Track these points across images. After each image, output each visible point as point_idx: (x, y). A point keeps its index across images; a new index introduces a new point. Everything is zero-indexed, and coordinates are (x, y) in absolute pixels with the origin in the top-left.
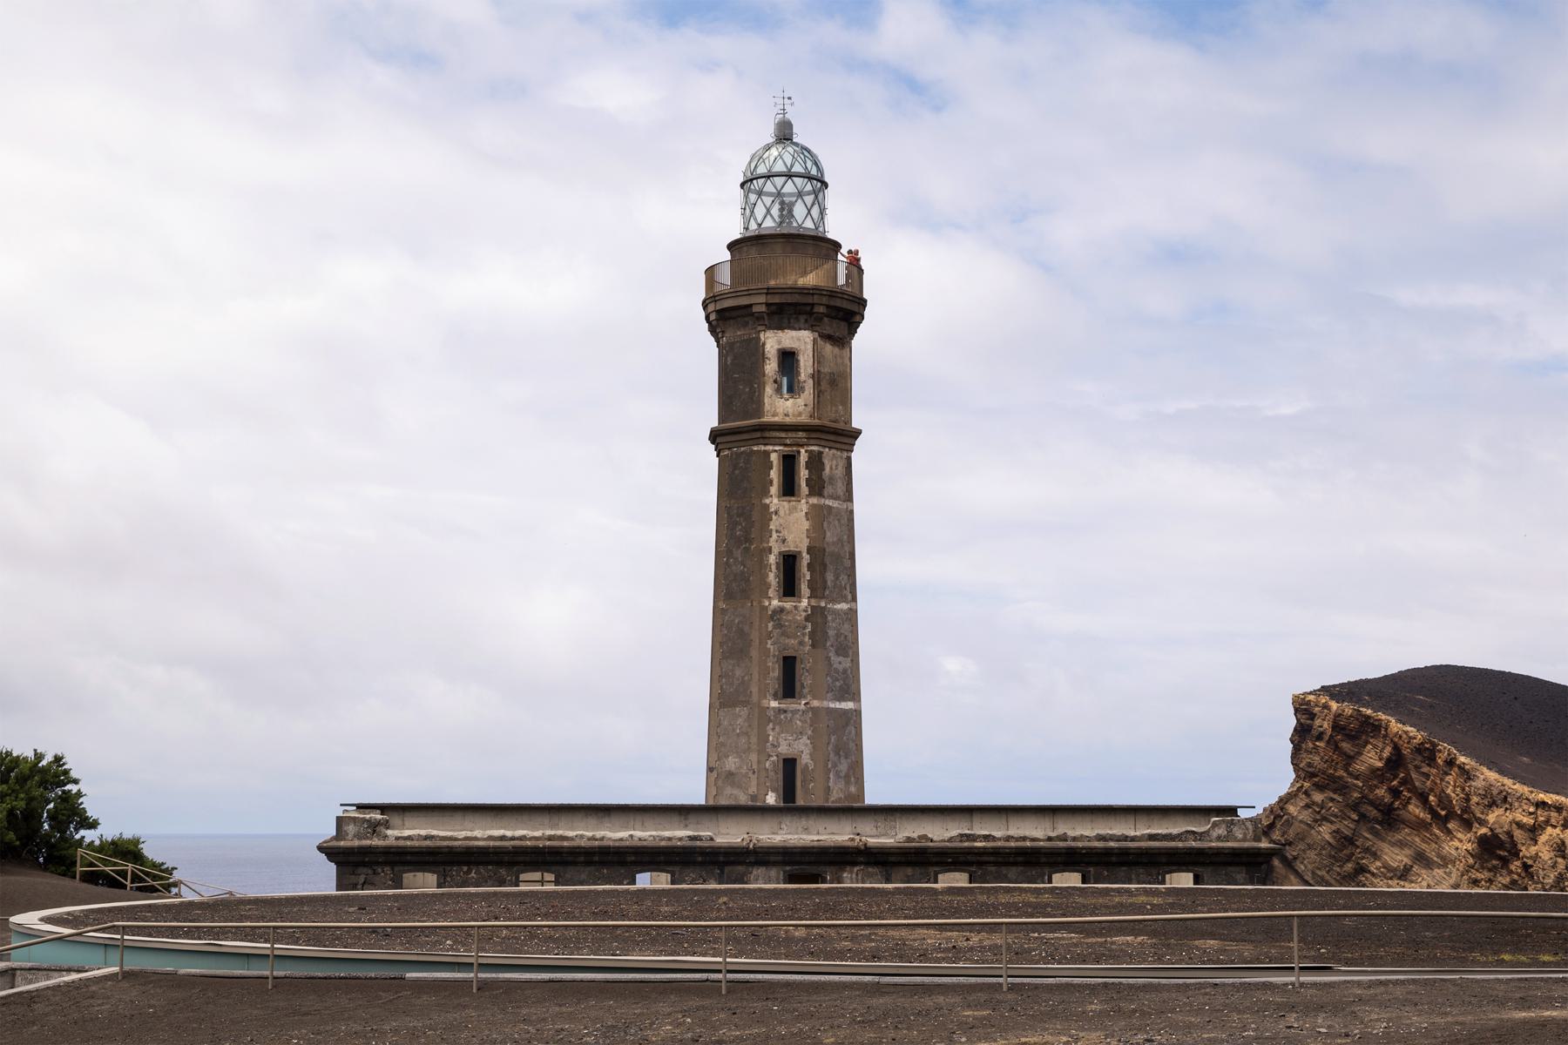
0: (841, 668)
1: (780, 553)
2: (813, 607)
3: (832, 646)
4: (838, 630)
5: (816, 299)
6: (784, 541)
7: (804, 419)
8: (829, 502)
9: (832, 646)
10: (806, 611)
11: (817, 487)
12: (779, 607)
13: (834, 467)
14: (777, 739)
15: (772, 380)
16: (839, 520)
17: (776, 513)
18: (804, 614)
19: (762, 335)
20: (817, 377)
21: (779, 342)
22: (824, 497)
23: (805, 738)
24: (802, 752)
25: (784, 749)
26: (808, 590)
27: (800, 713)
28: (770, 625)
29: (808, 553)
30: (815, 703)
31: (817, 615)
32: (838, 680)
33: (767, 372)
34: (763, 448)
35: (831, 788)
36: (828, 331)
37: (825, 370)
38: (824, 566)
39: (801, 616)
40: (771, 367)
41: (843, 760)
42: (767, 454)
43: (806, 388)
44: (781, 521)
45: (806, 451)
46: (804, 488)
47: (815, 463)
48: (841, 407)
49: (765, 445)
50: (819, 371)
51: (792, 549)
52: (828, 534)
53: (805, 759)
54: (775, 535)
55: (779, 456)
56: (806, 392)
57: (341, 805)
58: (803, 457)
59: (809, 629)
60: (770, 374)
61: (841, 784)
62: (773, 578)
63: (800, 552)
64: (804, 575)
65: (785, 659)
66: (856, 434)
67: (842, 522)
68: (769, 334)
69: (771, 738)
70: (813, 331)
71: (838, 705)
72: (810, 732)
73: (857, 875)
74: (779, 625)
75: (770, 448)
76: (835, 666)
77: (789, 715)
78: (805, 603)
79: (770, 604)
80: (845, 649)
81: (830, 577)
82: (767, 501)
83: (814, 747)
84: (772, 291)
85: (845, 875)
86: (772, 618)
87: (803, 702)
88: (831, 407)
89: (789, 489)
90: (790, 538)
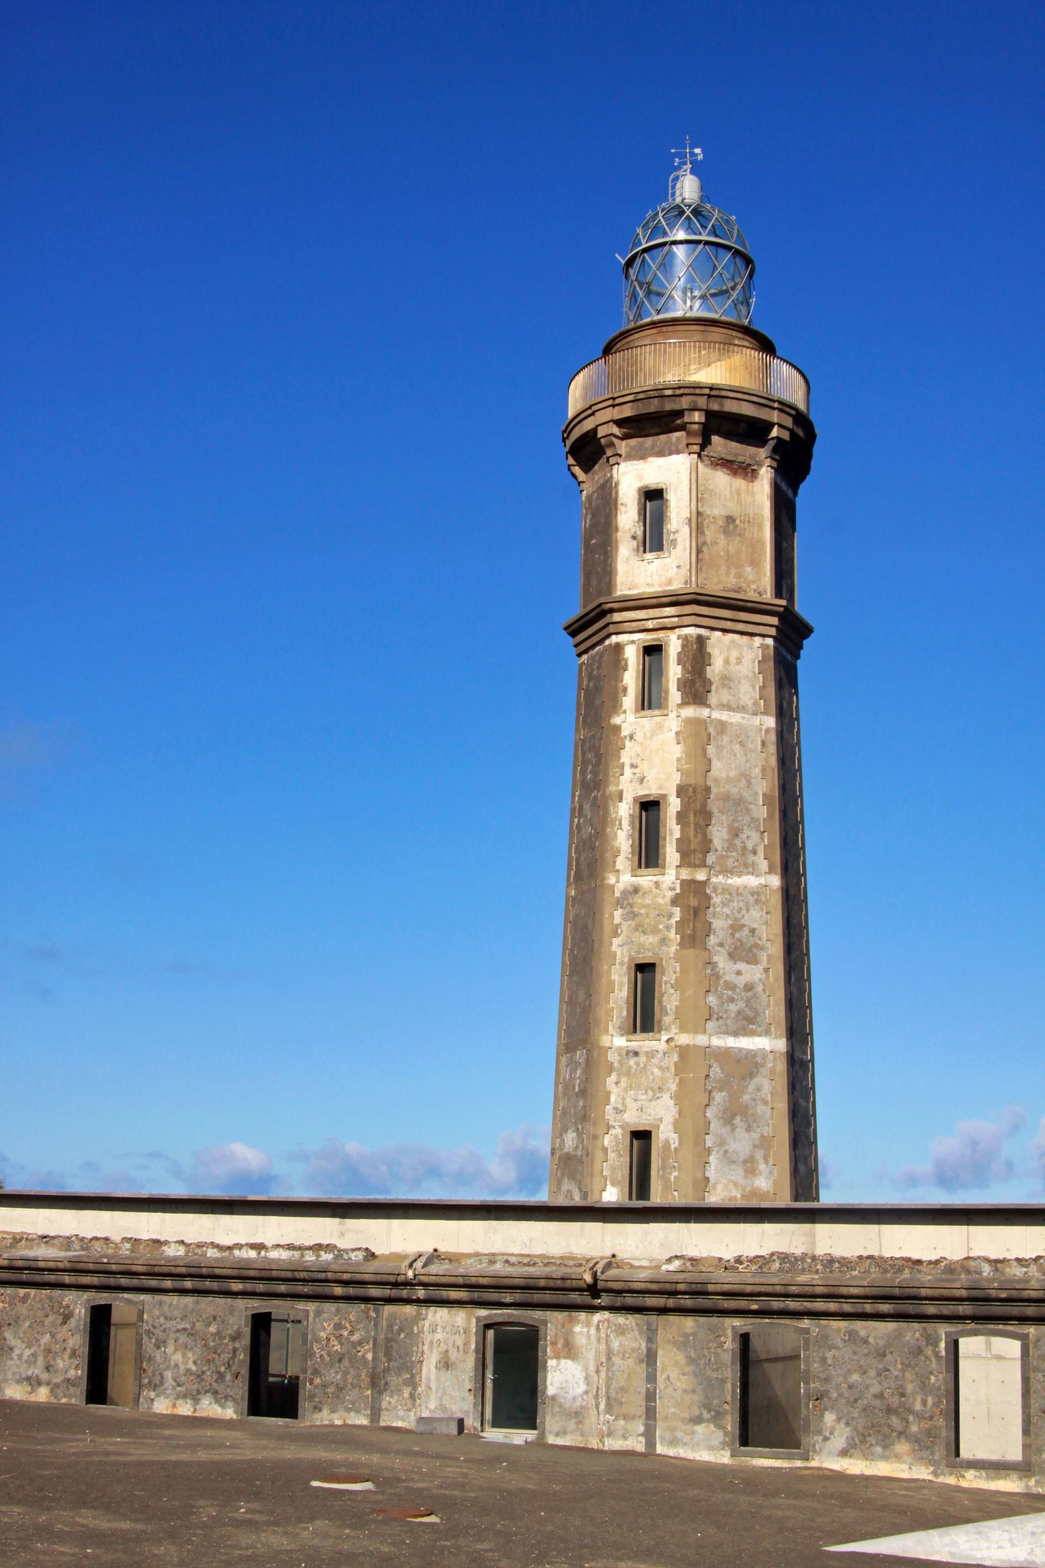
0: (741, 981)
1: (635, 800)
2: (685, 883)
3: (721, 945)
4: (736, 919)
5: (684, 403)
6: (642, 780)
7: (677, 586)
8: (724, 716)
9: (721, 945)
10: (673, 889)
12: (632, 885)
13: (733, 660)
14: (624, 1099)
15: (628, 536)
16: (742, 744)
18: (670, 894)
20: (698, 522)
21: (641, 478)
22: (709, 706)
23: (666, 1096)
24: (661, 1120)
26: (678, 855)
27: (660, 1056)
30: (684, 1039)
32: (732, 1000)
35: (712, 1181)
37: (716, 510)
38: (706, 816)
39: (664, 897)
41: (741, 1133)
42: (619, 648)
43: (679, 540)
44: (639, 749)
45: (679, 637)
46: (675, 695)
48: (749, 569)
52: (717, 765)
53: (665, 1135)
54: (628, 772)
55: (638, 650)
56: (680, 547)
59: (677, 917)
60: (627, 528)
61: (737, 1174)
63: (664, 796)
64: (672, 830)
67: (751, 746)
69: (613, 1098)
71: (731, 1042)
72: (673, 1087)
73: (598, 1328)
74: (632, 915)
76: (727, 978)
77: (642, 1059)
79: (618, 882)
80: (750, 950)
81: (718, 834)
82: (616, 720)
83: (680, 1113)
84: (618, 401)
85: (577, 1329)
87: (664, 1038)
88: (729, 568)
90: (650, 777)
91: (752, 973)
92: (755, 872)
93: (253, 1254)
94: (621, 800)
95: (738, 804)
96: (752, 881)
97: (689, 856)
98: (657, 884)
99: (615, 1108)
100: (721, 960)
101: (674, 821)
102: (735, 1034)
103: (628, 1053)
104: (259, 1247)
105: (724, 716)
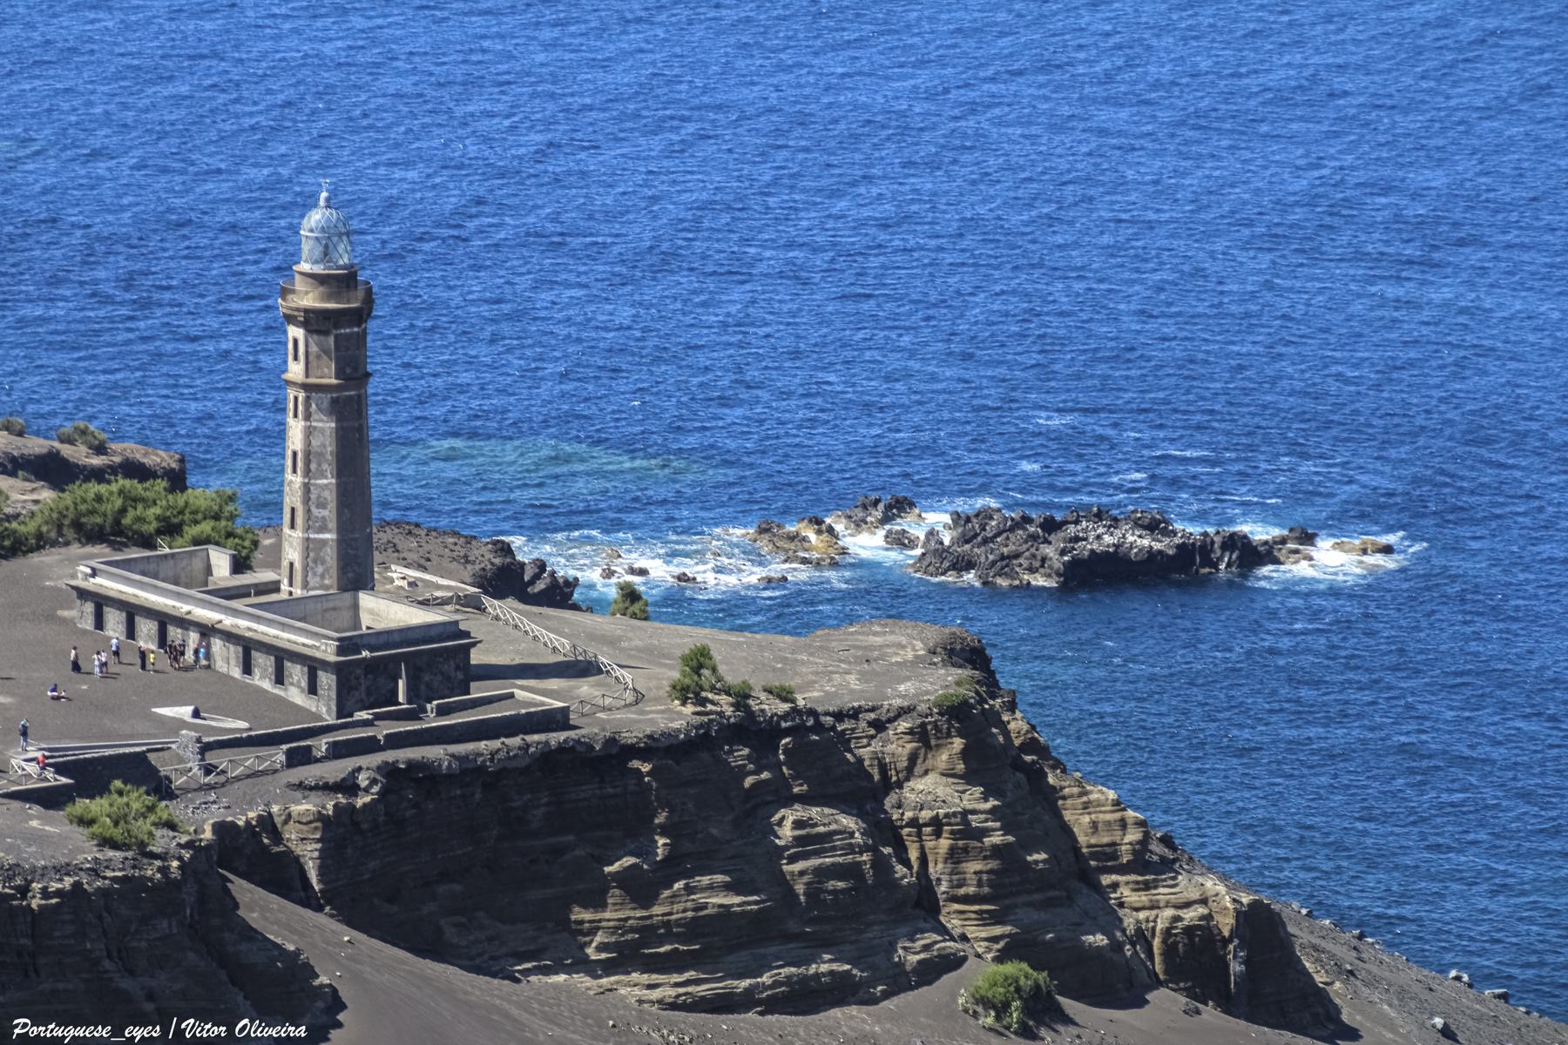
11: (308, 417)
36: (315, 327)
40: (290, 346)
61: (318, 579)
71: (316, 536)
81: (313, 466)
89: (296, 416)
91: (325, 513)
92: (326, 478)
95: (321, 455)
96: (325, 481)
100: (313, 509)
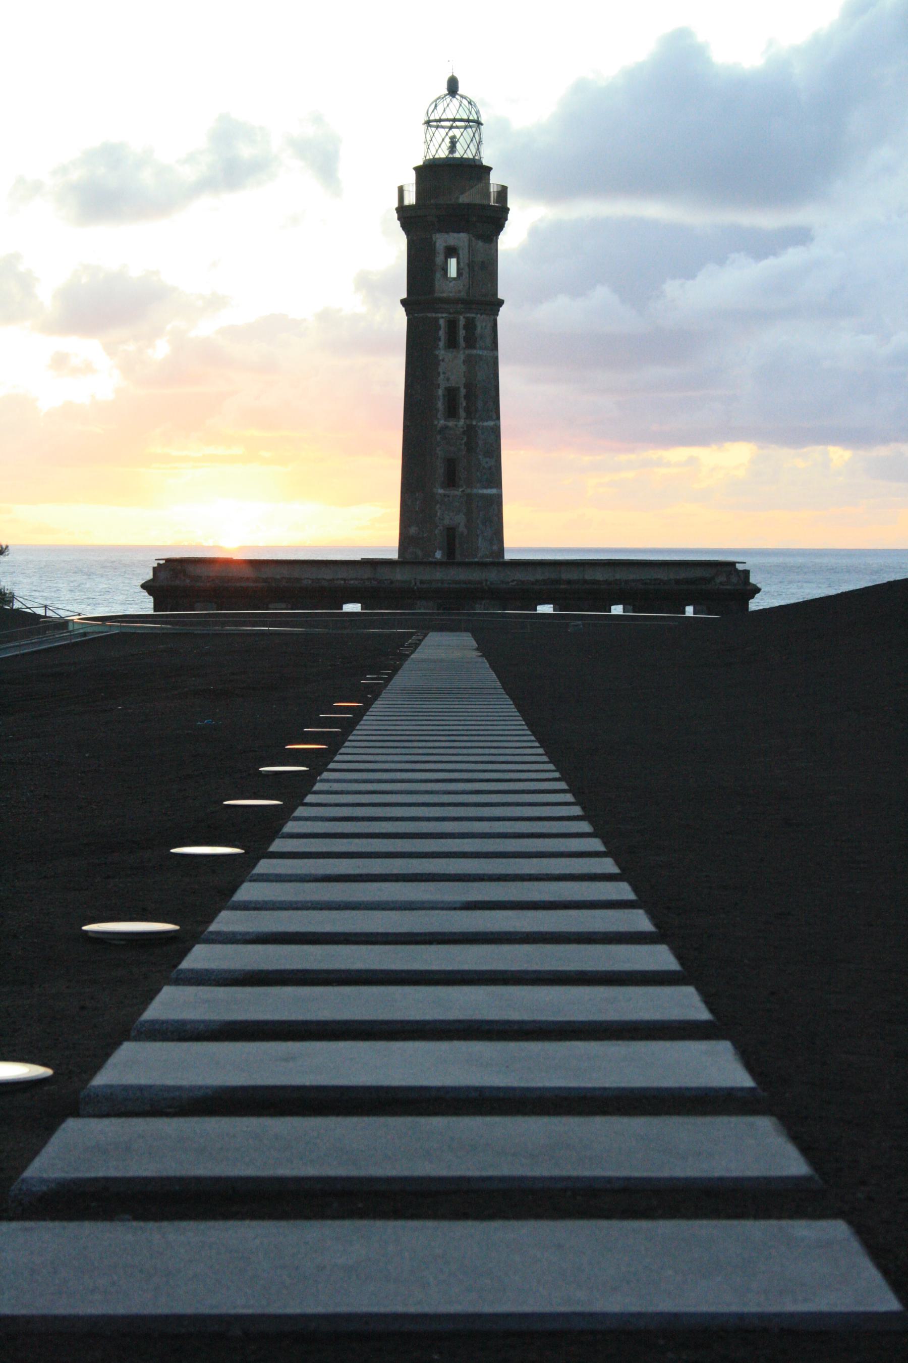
1: (446, 388)
2: (468, 426)
6: (448, 379)
7: (463, 294)
8: (480, 352)
10: (463, 428)
12: (445, 425)
17: (443, 360)
18: (461, 430)
19: (434, 237)
25: (447, 522)
28: (439, 437)
29: (464, 387)
30: (469, 491)
31: (470, 431)
33: (437, 263)
34: (434, 315)
42: (437, 319)
45: (464, 317)
46: (462, 343)
47: (470, 326)
49: (436, 313)
50: (472, 261)
51: (453, 385)
53: (462, 529)
54: (442, 376)
57: (156, 560)
58: (462, 321)
60: (440, 264)
62: (440, 405)
65: (448, 460)
66: (501, 303)
68: (438, 235)
69: (438, 514)
70: (468, 233)
71: (486, 491)
75: (440, 315)
78: (462, 422)
79: (438, 422)
81: (480, 404)
85: (477, 606)
86: (440, 432)
87: (461, 490)
89: (452, 343)
93: (342, 582)
94: (439, 388)
97: (470, 414)
98: (456, 425)
99: (439, 518)
101: (463, 399)
102: (486, 488)
103: (445, 495)
104: (345, 580)
105: (480, 352)
